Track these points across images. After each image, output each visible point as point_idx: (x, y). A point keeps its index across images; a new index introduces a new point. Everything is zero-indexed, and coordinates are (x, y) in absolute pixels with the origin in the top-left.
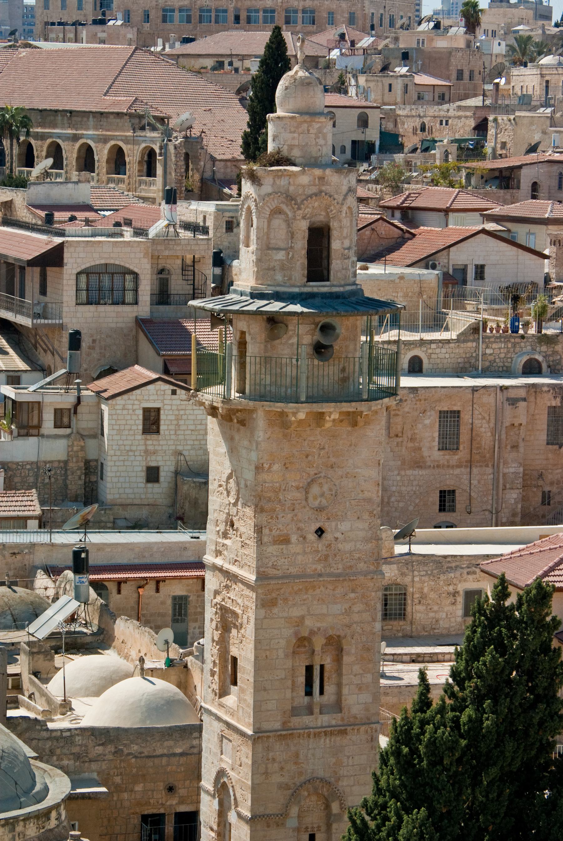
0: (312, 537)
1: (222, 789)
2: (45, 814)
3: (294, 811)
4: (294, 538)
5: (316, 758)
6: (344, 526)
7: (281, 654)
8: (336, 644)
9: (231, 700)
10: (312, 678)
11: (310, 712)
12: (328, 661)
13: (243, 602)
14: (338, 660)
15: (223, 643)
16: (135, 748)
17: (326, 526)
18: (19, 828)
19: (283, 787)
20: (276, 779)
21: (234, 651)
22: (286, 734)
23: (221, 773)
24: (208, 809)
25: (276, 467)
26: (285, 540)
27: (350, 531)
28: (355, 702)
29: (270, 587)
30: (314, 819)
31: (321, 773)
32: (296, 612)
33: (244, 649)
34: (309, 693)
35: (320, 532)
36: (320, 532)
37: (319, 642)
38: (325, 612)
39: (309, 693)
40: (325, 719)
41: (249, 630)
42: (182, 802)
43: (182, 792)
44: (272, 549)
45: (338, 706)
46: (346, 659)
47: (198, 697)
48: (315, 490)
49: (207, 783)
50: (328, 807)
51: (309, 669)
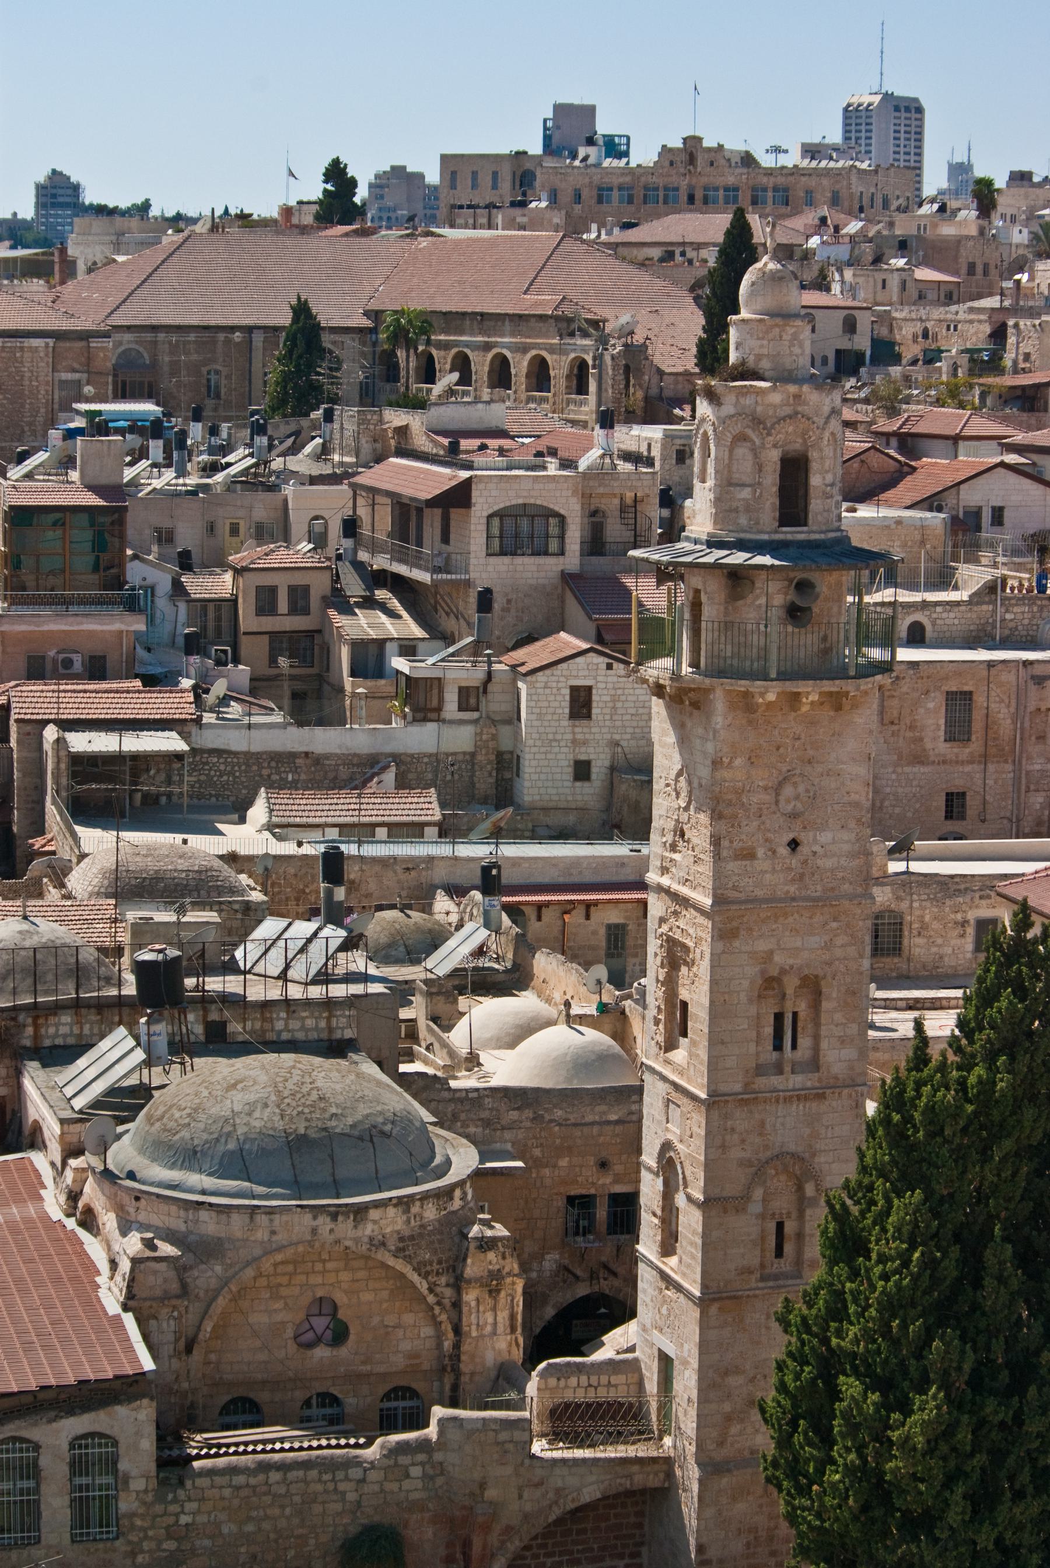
0: (784, 851)
1: (668, 1166)
2: (447, 1193)
3: (758, 1193)
4: (760, 852)
5: (786, 1127)
6: (825, 837)
7: (743, 997)
8: (813, 987)
9: (679, 1055)
11: (779, 1069)
12: (803, 1007)
13: (696, 932)
14: (816, 1006)
15: (670, 984)
16: (559, 1113)
17: (803, 837)
18: (415, 1209)
19: (743, 1163)
20: (736, 1153)
21: (684, 994)
22: (749, 1098)
23: (667, 1146)
24: (650, 1190)
25: (738, 762)
27: (832, 843)
28: (836, 1058)
29: (729, 914)
30: (784, 1203)
31: (792, 1147)
32: (762, 946)
33: (696, 992)
34: (778, 1047)
35: (794, 844)
36: (794, 844)
37: (791, 984)
39: (778, 1047)
40: (797, 1080)
41: (703, 968)
42: (617, 1180)
43: (618, 1168)
44: (732, 866)
45: (814, 1064)
46: (825, 1005)
47: (638, 1051)
48: (788, 791)
49: (649, 1158)
50: (800, 1188)
51: (779, 1017)
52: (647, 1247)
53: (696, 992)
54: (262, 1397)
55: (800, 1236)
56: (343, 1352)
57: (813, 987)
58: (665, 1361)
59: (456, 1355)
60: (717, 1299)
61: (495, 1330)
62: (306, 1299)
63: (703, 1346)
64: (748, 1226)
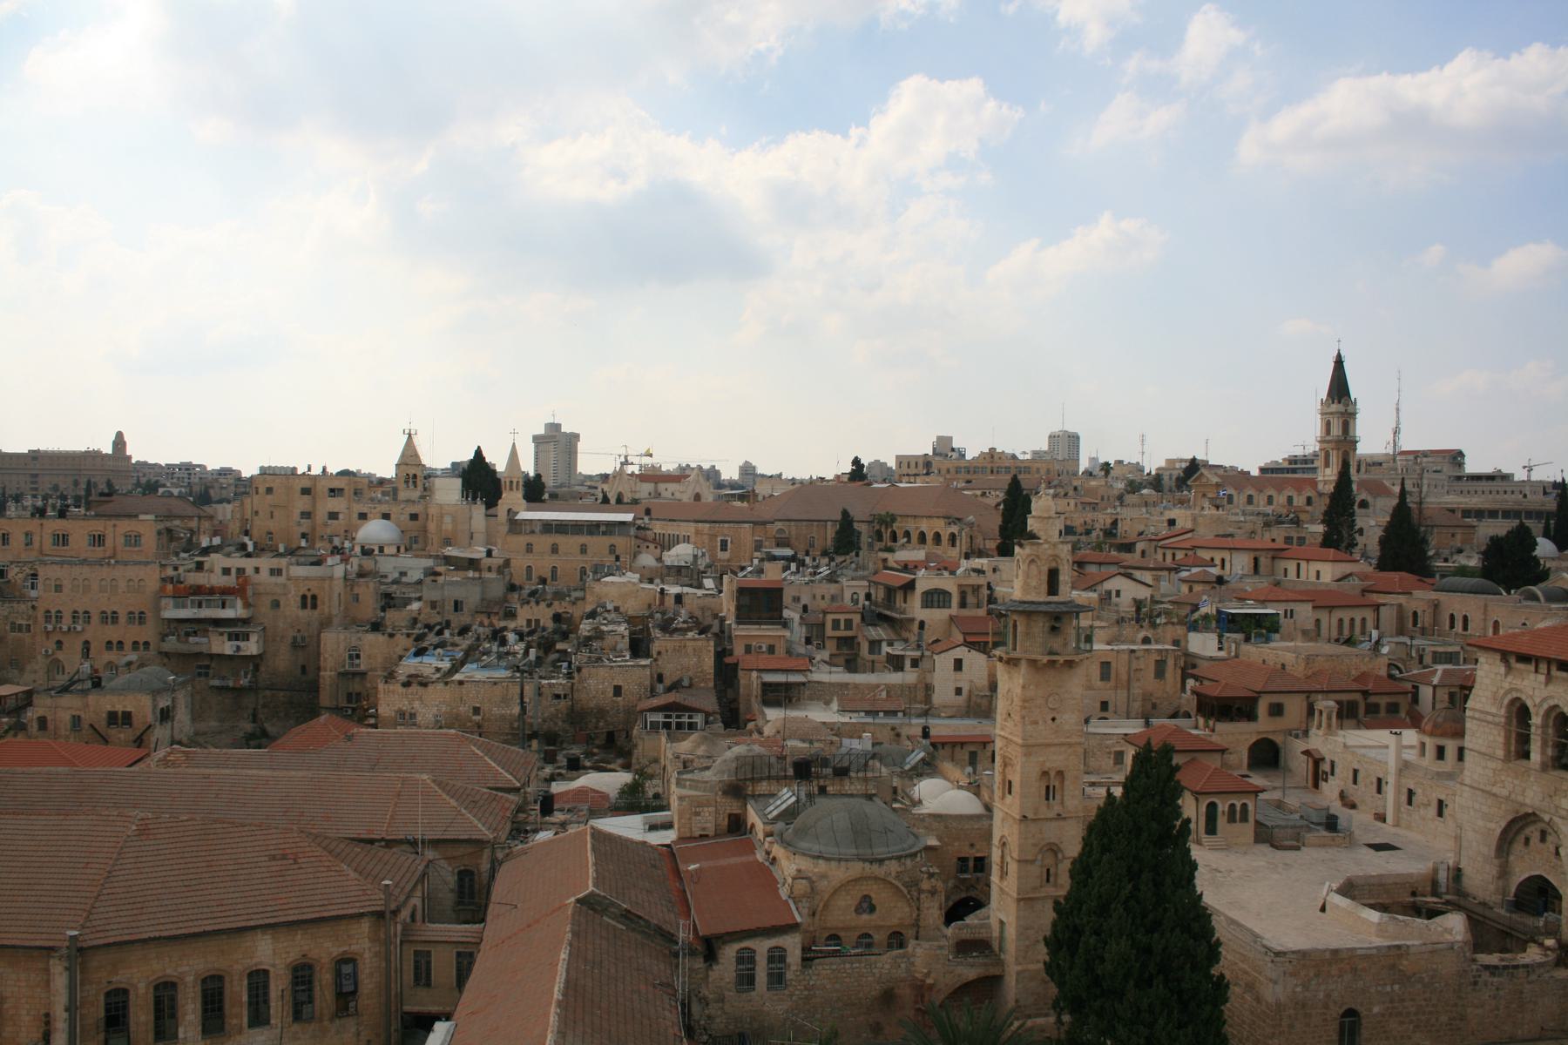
5: (1051, 832)
6: (1066, 717)
8: (1060, 773)
10: (1049, 793)
12: (1057, 784)
13: (1015, 753)
14: (1062, 782)
15: (1003, 773)
19: (1035, 845)
21: (1010, 777)
26: (1036, 723)
29: (1029, 748)
37: (1052, 774)
38: (1055, 760)
44: (1029, 727)
49: (996, 841)
52: (995, 878)
53: (1016, 780)
54: (842, 934)
55: (1056, 875)
56: (874, 916)
57: (1060, 773)
58: (1002, 922)
59: (917, 920)
60: (1025, 900)
61: (933, 913)
62: (860, 895)
63: (1018, 918)
64: (1036, 870)
